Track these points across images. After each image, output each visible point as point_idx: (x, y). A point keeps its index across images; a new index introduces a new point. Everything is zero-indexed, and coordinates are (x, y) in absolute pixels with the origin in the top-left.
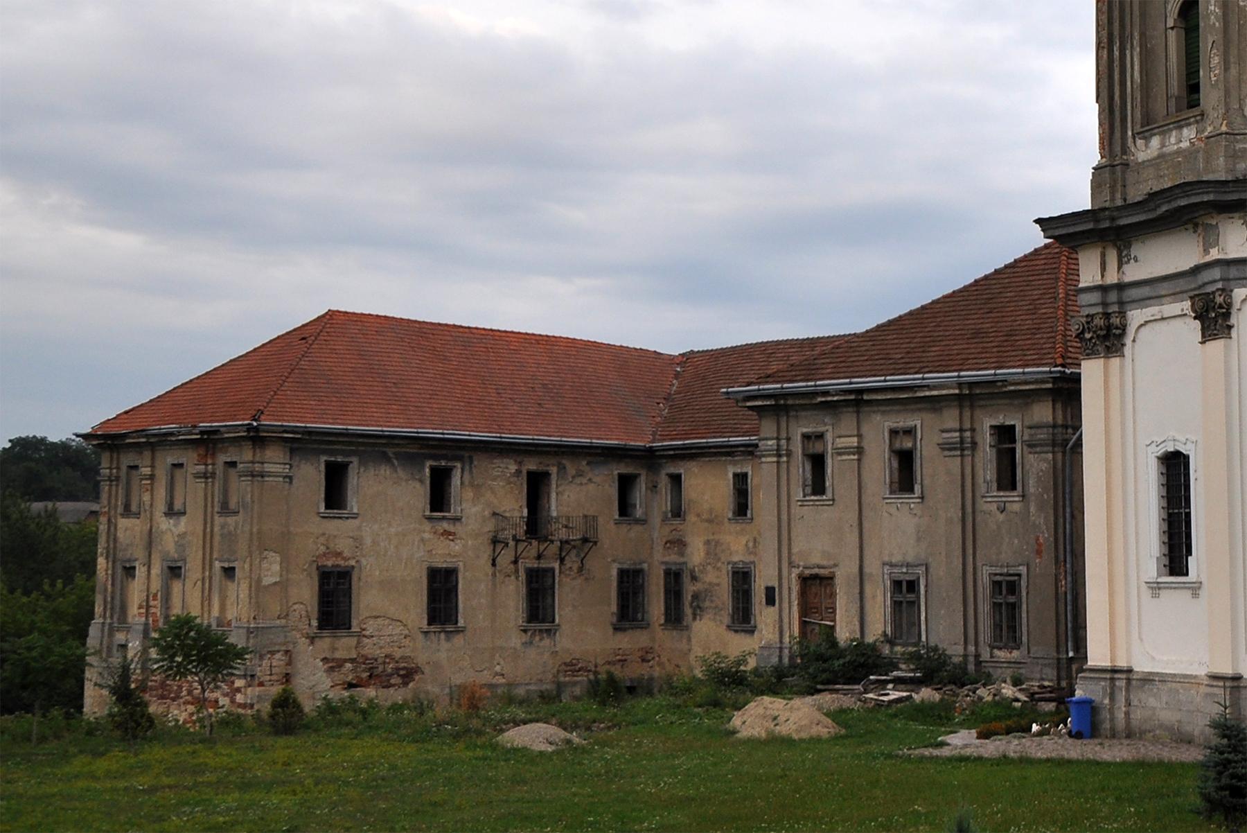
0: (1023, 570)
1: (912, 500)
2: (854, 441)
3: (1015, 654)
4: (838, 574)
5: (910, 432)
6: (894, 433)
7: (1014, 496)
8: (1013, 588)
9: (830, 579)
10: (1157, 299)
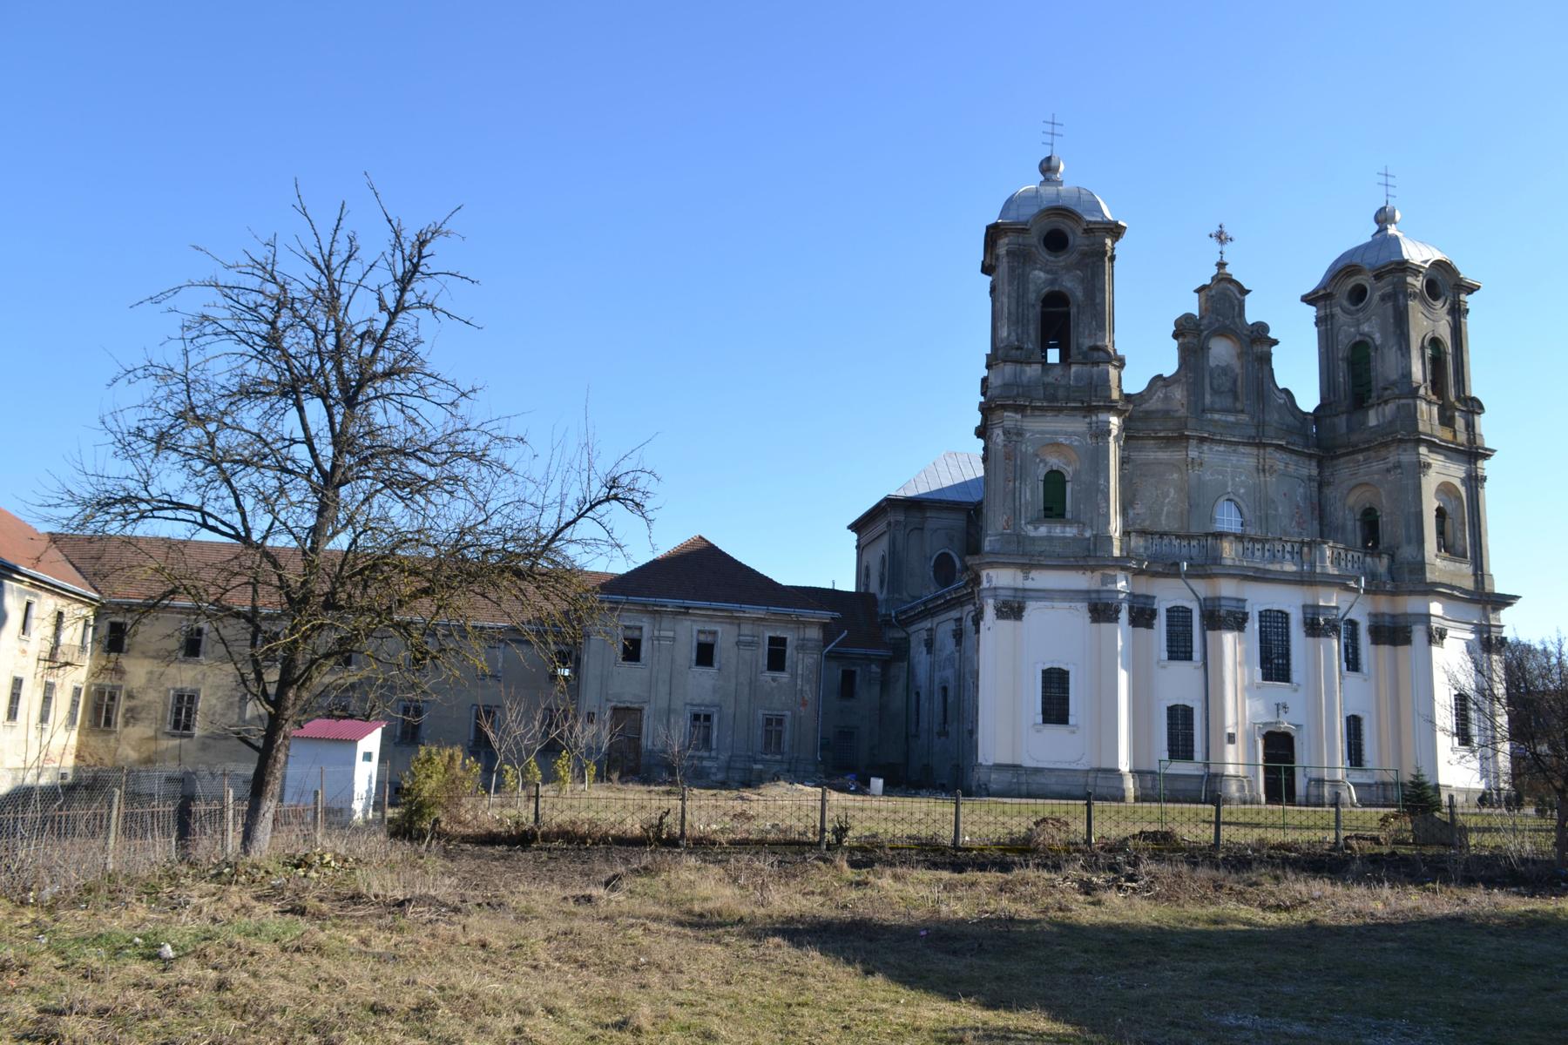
0: (788, 713)
1: (711, 671)
2: (671, 634)
3: (778, 757)
4: (647, 707)
5: (715, 633)
6: (700, 632)
7: (784, 677)
8: (780, 722)
9: (640, 710)
10: (1052, 599)
